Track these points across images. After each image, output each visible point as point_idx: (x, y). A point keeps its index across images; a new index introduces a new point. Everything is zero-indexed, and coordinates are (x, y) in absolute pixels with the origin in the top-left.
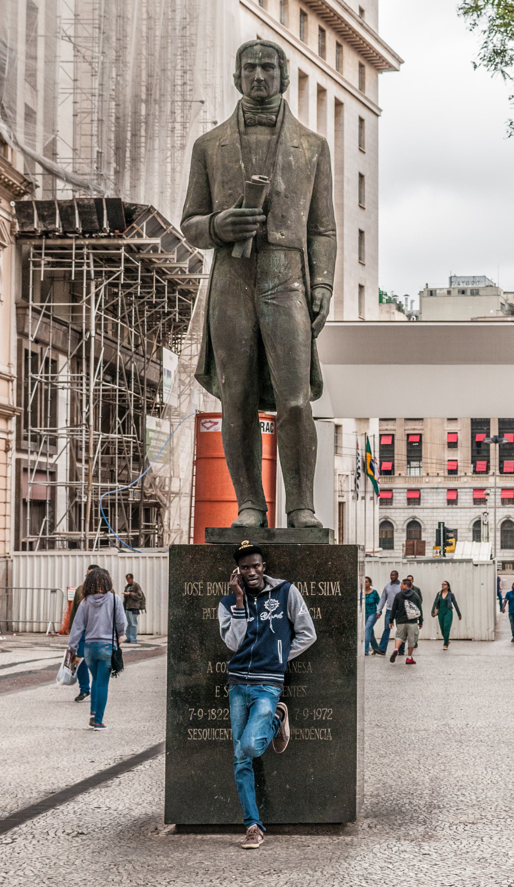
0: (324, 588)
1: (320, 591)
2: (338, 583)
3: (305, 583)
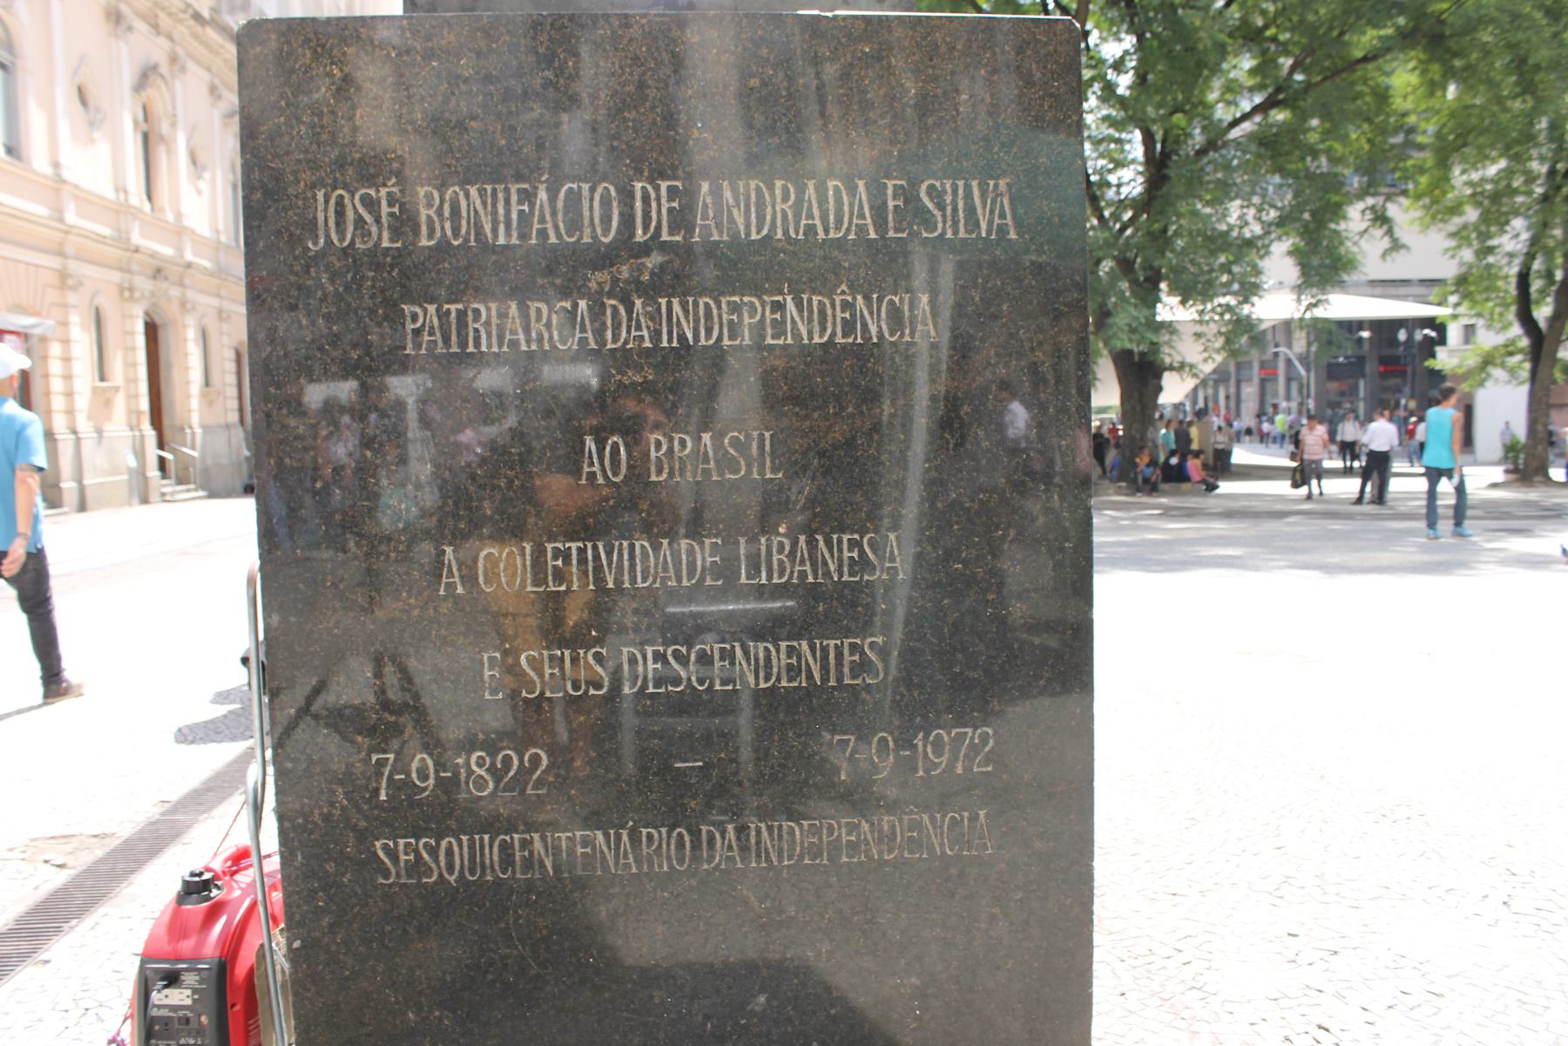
0: (941, 207)
1: (929, 224)
2: (1002, 183)
3: (861, 185)
